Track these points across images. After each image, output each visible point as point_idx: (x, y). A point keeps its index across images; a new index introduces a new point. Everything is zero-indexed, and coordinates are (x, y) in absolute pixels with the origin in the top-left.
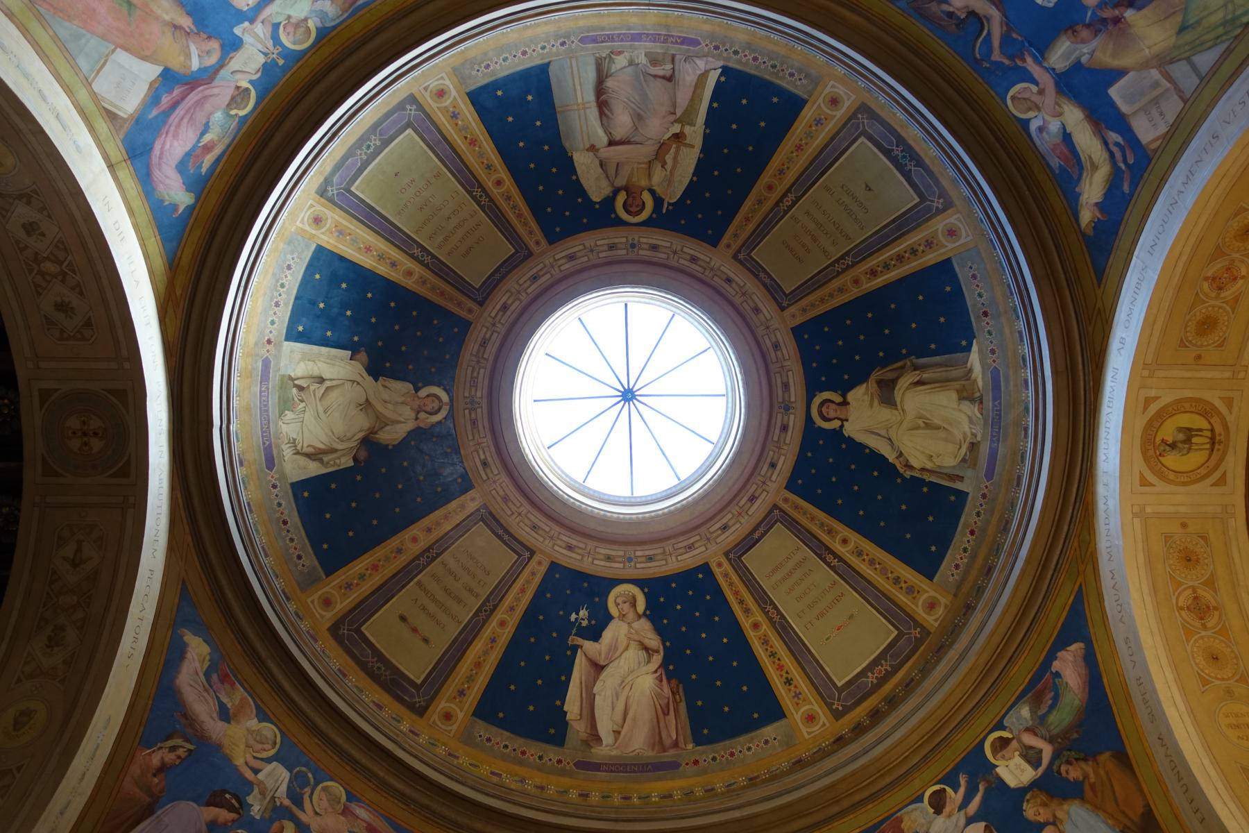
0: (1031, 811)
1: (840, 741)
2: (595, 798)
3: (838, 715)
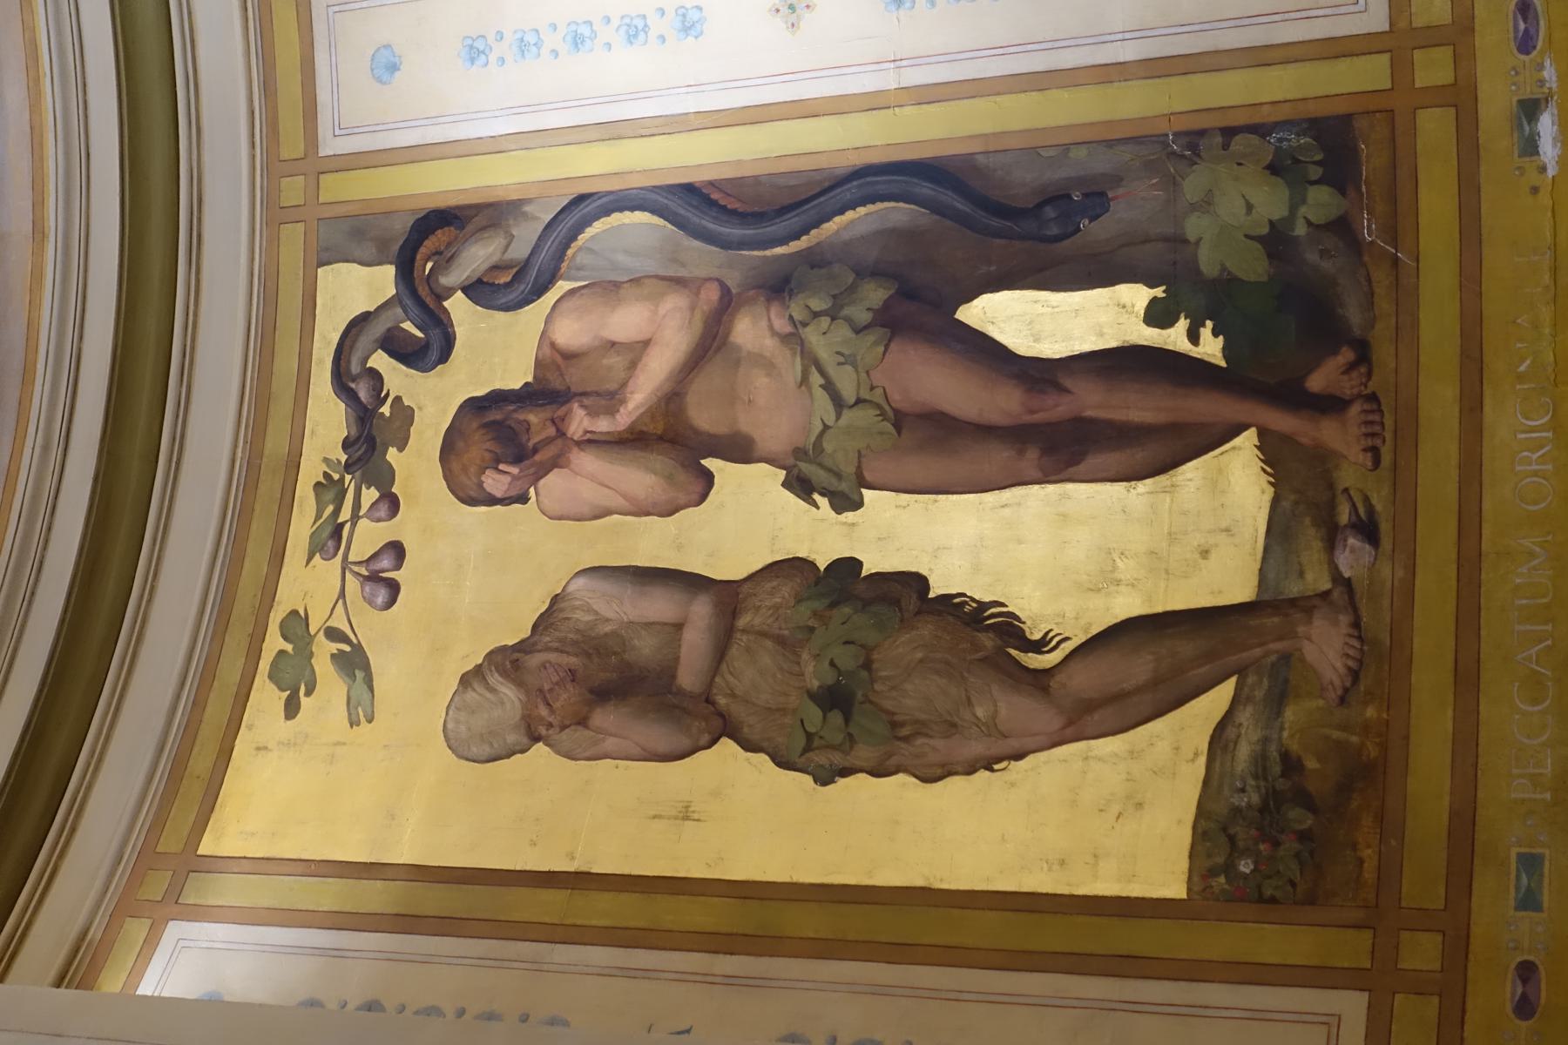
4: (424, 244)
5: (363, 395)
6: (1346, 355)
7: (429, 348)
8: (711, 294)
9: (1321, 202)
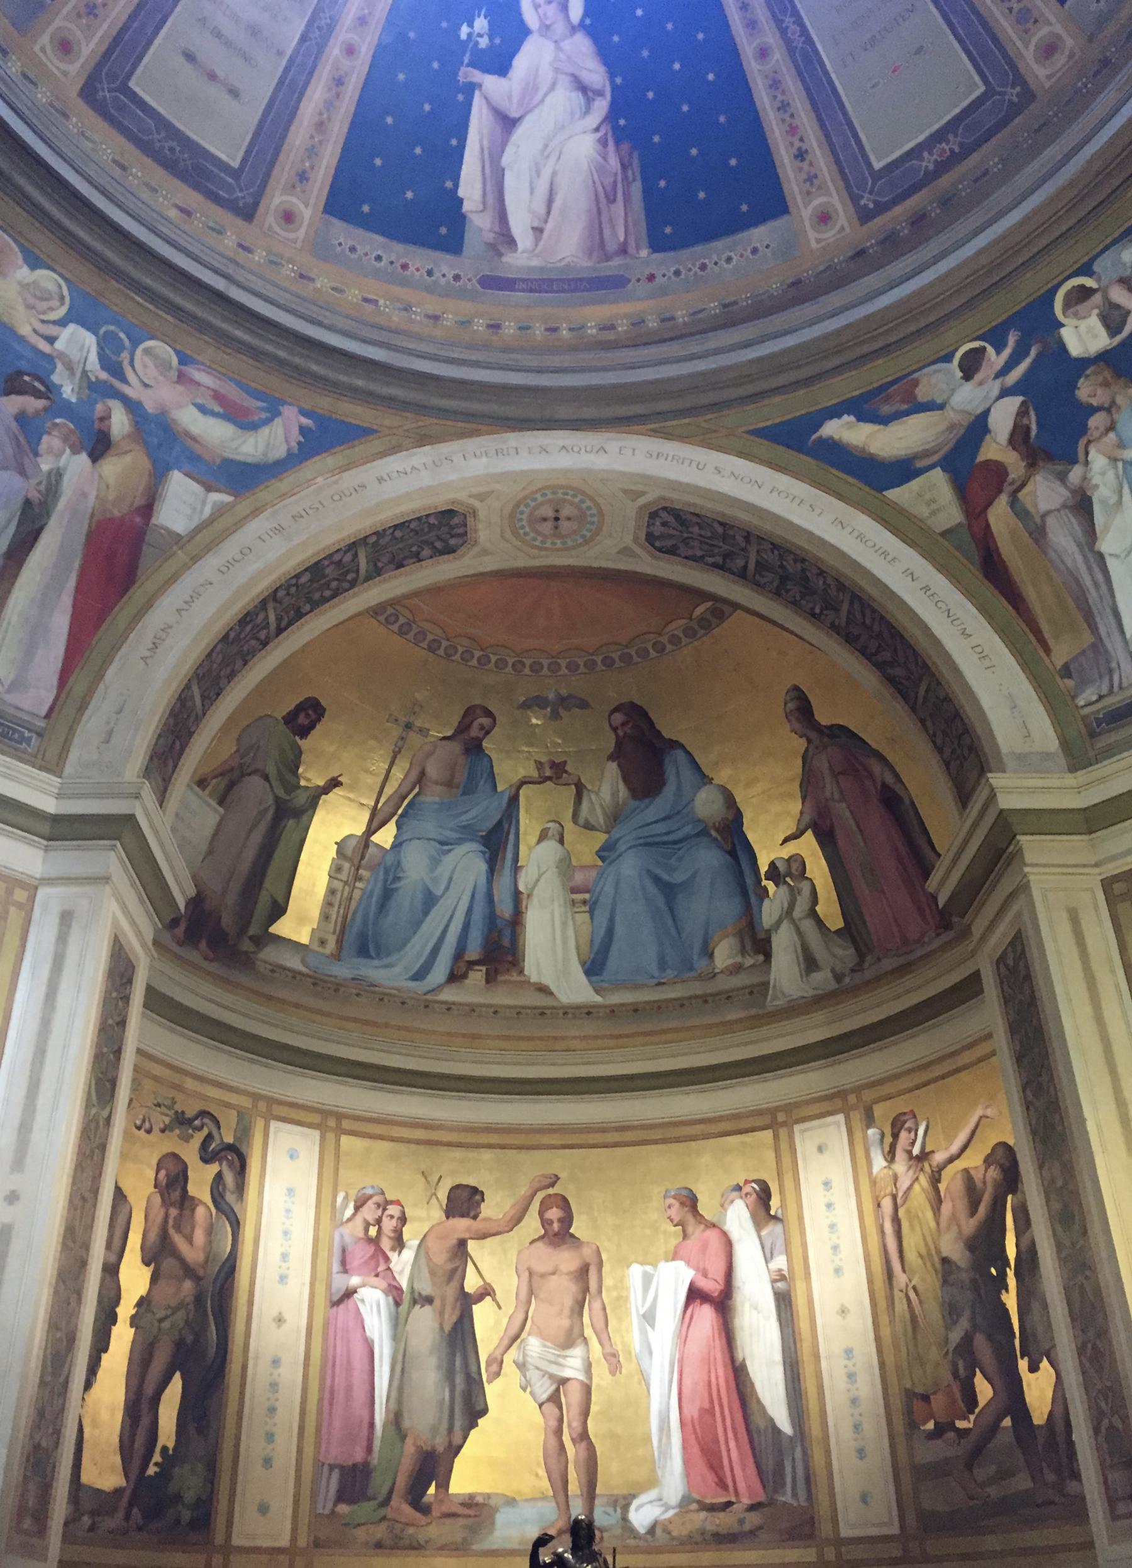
0: (1086, 391)
1: (861, 260)
2: (509, 329)
3: (865, 216)
4: (235, 1157)
5: (197, 1122)
6: (140, 1522)
7: (207, 1157)
8: (201, 1273)
9: (186, 1515)
